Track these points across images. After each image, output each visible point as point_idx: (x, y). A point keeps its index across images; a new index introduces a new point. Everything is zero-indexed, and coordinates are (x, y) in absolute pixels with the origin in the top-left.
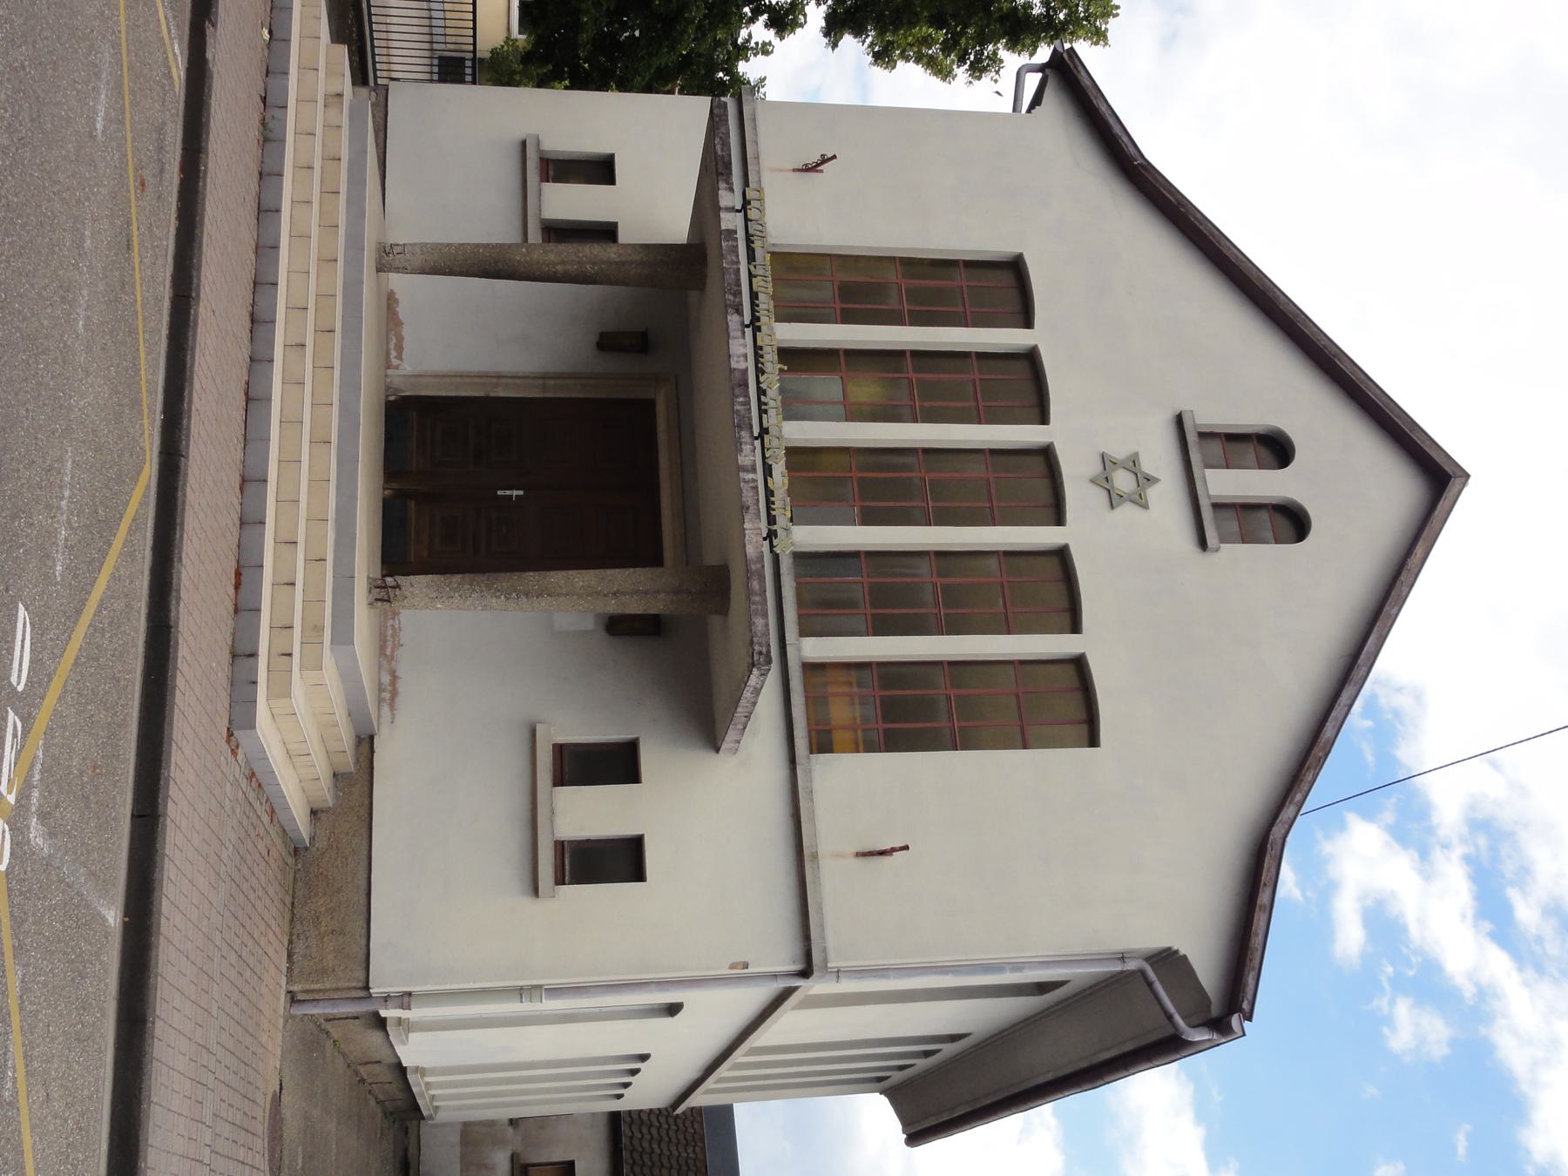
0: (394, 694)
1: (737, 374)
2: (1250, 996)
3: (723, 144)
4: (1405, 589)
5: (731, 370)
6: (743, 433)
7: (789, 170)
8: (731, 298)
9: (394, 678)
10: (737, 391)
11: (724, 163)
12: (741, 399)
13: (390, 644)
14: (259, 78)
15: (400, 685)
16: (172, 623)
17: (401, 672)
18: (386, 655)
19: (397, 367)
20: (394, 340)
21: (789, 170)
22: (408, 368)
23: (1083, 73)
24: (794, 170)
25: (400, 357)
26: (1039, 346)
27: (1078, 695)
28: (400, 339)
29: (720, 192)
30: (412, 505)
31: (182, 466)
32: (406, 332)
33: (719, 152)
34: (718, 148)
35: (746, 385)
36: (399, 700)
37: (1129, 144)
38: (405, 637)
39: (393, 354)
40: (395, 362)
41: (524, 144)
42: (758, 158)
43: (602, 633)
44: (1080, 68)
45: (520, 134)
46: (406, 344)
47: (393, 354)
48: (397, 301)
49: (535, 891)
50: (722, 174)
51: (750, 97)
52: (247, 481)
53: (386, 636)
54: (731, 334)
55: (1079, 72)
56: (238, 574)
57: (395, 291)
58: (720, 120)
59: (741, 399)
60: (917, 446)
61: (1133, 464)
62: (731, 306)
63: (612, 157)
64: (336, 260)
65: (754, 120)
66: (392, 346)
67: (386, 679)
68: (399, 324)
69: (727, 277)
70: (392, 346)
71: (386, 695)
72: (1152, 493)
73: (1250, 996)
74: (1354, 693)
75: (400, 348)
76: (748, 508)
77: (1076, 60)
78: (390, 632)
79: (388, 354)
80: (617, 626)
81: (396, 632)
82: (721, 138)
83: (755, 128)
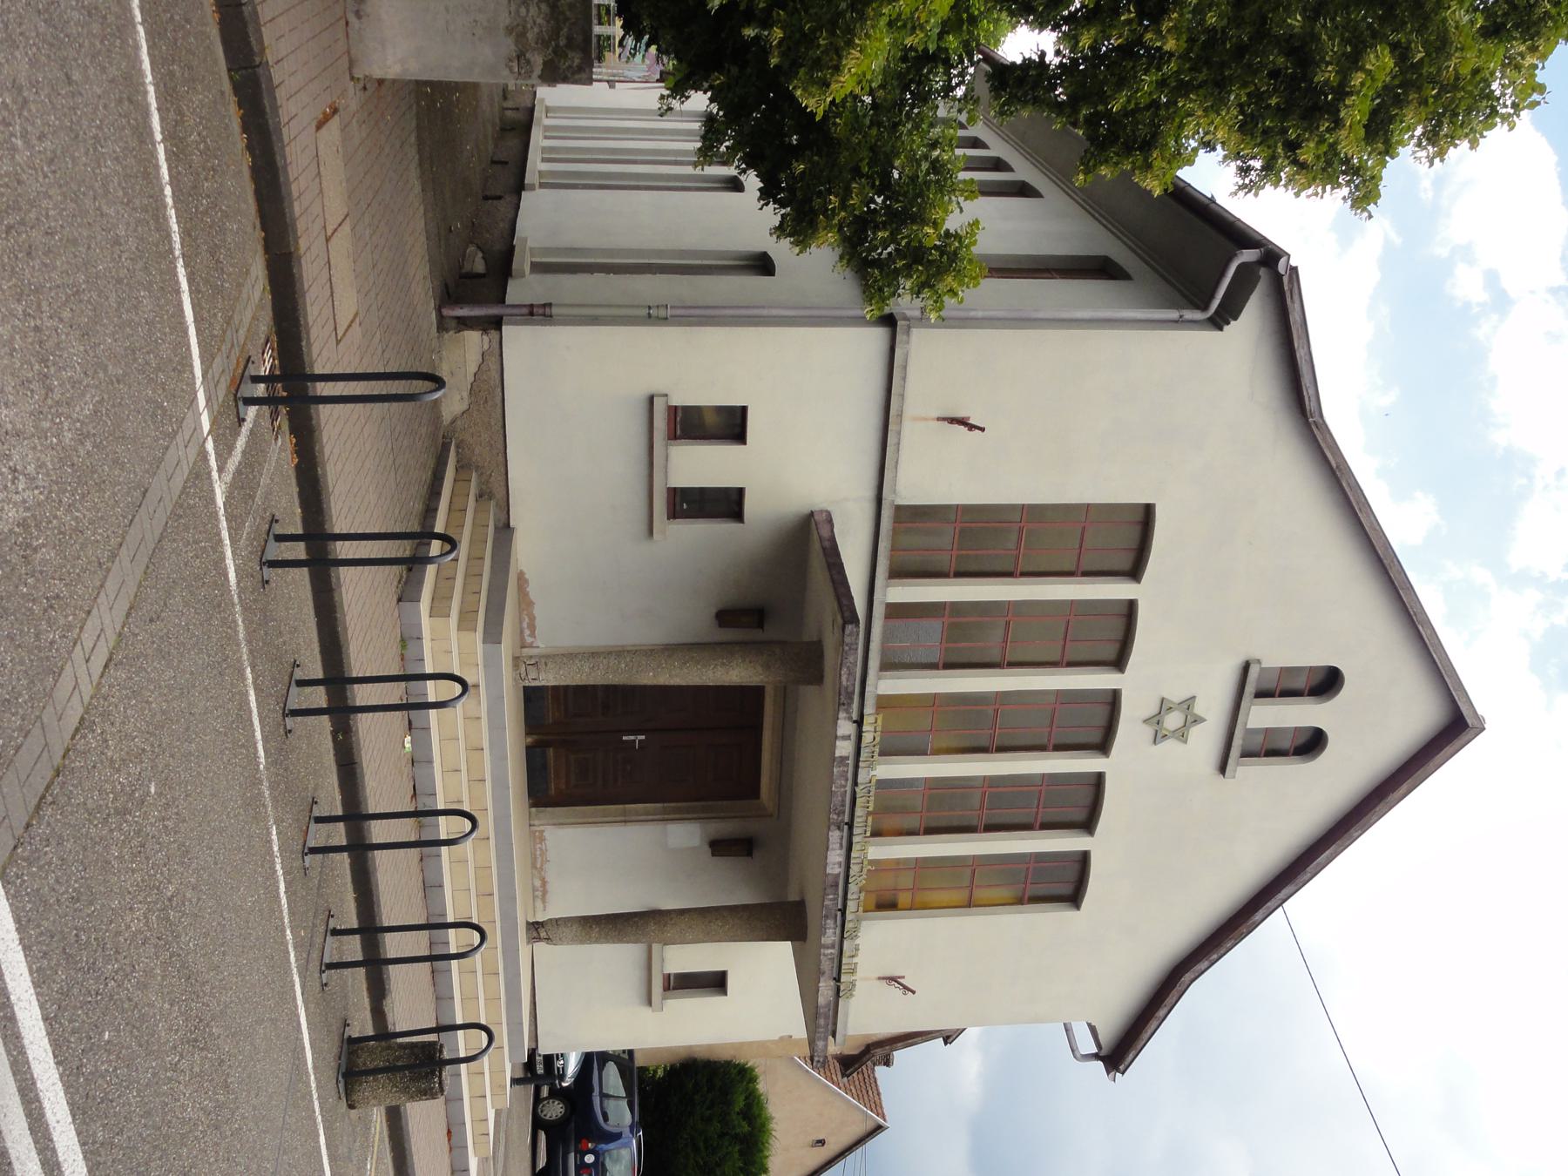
0: (545, 893)
1: (830, 878)
2: (1127, 1063)
3: (849, 674)
4: (1375, 818)
5: (827, 875)
6: (828, 921)
7: (933, 419)
8: (835, 817)
9: (544, 883)
10: (828, 891)
11: (847, 693)
12: (831, 897)
13: (539, 861)
14: (407, 769)
15: (550, 887)
16: (334, 587)
17: (550, 878)
18: (536, 868)
19: (531, 646)
20: (527, 620)
21: (933, 419)
22: (542, 646)
23: (1297, 305)
24: (938, 419)
25: (533, 635)
26: (1139, 603)
27: (1108, 708)
28: (532, 619)
29: (839, 721)
30: (551, 752)
31: (314, 416)
32: (537, 611)
33: (844, 683)
34: (844, 678)
35: (837, 885)
36: (548, 896)
37: (1313, 399)
38: (551, 855)
39: (527, 632)
40: (529, 640)
41: (651, 400)
42: (901, 416)
43: (708, 850)
44: (1296, 297)
45: (642, 389)
46: (538, 622)
47: (527, 632)
48: (526, 581)
49: (650, 1003)
50: (844, 704)
51: (905, 337)
52: (441, 999)
53: (535, 855)
54: (831, 847)
55: (1293, 302)
56: (449, 1132)
57: (525, 570)
58: (850, 649)
59: (831, 897)
60: (984, 835)
61: (1188, 703)
62: (833, 823)
63: (744, 409)
64: (488, 838)
65: (905, 368)
66: (525, 625)
67: (538, 883)
68: (531, 604)
69: (834, 799)
70: (525, 625)
71: (539, 893)
72: (1195, 732)
73: (1127, 1063)
74: (1291, 892)
75: (532, 627)
76: (824, 973)
77: (1295, 284)
78: (538, 853)
79: (522, 632)
80: (719, 847)
81: (543, 853)
82: (848, 668)
83: (904, 379)
